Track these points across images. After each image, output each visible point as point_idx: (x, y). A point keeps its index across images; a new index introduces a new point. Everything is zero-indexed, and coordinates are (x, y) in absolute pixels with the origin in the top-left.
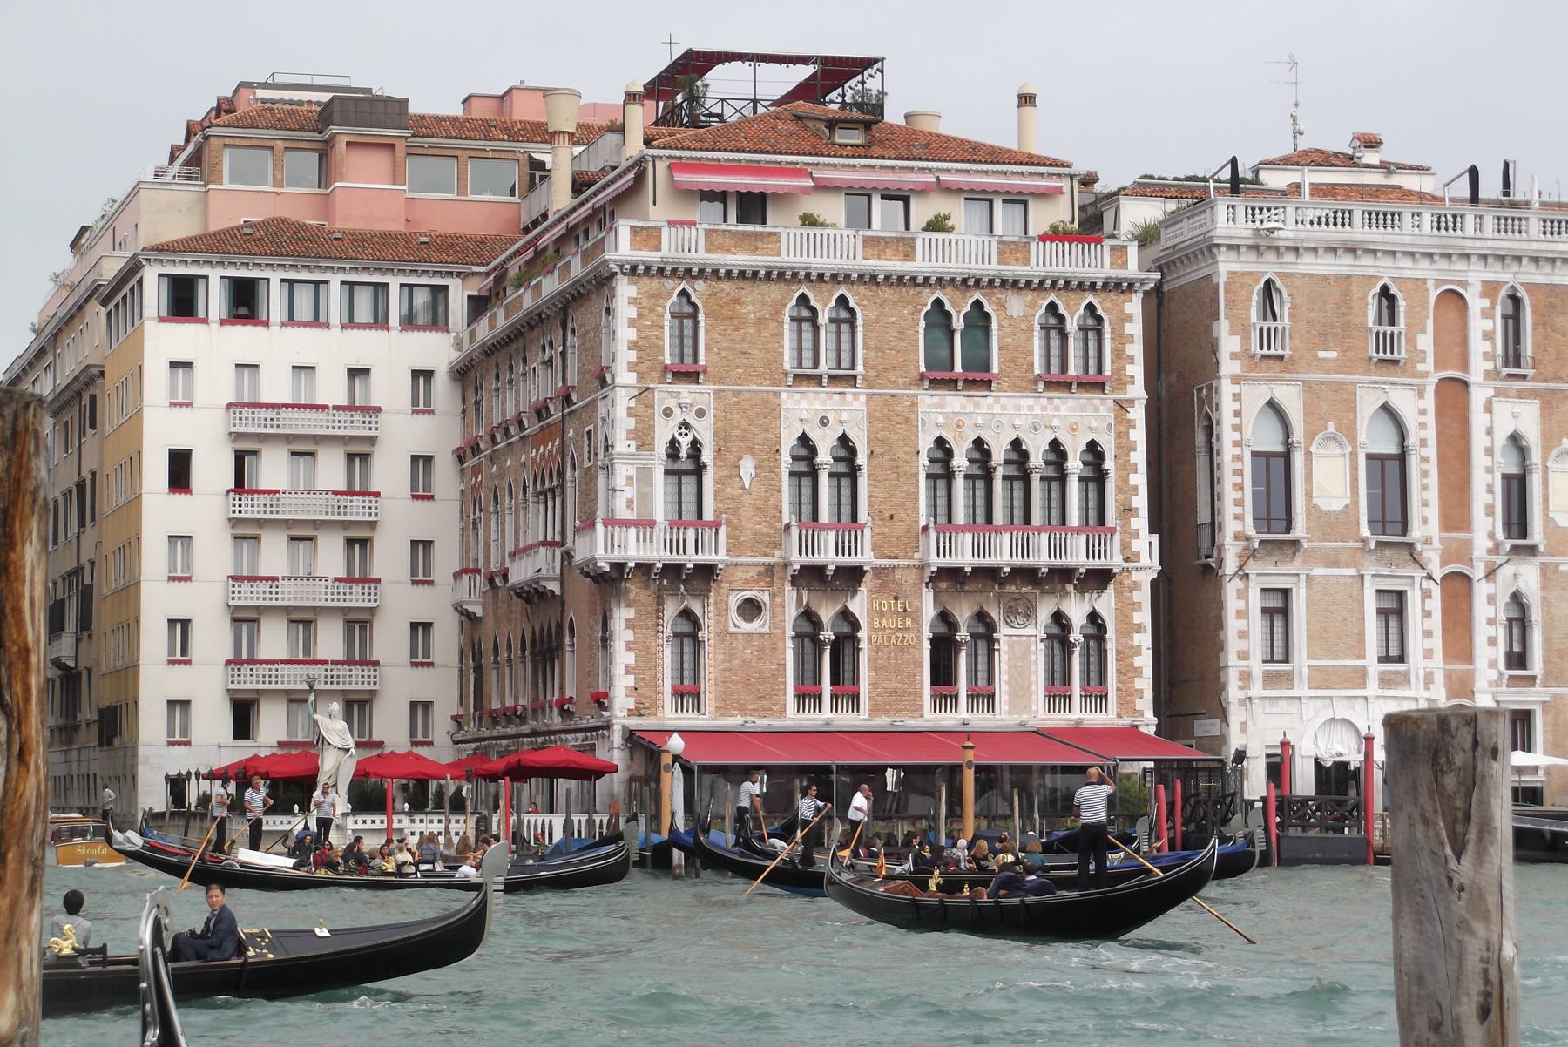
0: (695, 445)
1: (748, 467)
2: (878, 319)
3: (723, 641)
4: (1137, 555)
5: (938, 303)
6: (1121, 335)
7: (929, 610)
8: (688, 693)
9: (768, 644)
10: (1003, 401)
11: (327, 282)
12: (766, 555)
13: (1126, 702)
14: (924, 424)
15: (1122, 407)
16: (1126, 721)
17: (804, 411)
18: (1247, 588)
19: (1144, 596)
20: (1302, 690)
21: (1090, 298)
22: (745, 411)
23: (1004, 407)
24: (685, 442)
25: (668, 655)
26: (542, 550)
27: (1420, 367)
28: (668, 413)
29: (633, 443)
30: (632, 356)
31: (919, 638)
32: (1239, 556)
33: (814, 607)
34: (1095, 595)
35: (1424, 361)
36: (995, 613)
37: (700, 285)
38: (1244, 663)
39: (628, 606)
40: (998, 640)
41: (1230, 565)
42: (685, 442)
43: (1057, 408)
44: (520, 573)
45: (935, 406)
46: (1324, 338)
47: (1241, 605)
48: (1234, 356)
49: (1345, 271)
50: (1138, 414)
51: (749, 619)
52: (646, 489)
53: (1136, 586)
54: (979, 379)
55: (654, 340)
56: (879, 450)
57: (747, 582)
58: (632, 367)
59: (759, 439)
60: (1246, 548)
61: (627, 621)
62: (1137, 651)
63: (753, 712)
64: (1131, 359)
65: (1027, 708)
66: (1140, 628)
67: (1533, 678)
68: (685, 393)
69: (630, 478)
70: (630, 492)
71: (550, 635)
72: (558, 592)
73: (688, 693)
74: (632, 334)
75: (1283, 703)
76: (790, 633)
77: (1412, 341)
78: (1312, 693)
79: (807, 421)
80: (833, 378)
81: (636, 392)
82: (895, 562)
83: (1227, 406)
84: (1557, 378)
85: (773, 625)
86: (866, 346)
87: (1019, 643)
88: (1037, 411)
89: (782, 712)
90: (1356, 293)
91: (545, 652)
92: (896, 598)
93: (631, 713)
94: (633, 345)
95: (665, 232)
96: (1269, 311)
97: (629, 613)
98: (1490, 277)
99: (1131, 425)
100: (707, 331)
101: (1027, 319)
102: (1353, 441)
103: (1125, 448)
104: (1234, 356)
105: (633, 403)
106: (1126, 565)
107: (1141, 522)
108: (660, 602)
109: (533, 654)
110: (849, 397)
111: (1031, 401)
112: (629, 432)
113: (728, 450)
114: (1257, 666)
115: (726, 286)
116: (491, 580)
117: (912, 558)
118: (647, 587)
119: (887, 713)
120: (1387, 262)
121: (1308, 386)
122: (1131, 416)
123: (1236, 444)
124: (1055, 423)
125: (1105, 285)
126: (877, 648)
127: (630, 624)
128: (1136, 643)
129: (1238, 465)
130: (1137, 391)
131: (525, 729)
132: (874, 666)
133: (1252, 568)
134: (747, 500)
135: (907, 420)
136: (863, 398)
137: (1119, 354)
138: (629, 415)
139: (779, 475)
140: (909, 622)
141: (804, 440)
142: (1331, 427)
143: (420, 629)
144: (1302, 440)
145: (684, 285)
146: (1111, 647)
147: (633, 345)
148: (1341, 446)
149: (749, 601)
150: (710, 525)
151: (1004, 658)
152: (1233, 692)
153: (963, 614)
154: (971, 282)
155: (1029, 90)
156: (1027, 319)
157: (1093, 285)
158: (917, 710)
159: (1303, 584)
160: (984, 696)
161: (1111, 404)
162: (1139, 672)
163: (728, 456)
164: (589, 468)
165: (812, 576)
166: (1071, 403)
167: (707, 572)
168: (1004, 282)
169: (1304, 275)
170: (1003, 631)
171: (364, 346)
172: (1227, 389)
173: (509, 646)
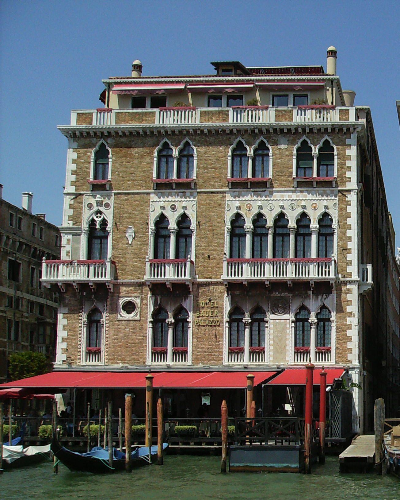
0: (104, 223)
1: (130, 233)
3: (114, 324)
4: (350, 274)
6: (344, 156)
7: (227, 307)
8: (93, 351)
15: (344, 193)
16: (341, 365)
24: (98, 220)
25: (84, 331)
28: (90, 206)
30: (73, 178)
31: (222, 321)
34: (324, 296)
39: (64, 306)
42: (98, 220)
50: (353, 198)
51: (129, 313)
52: (77, 246)
53: (349, 291)
57: (128, 293)
58: (73, 183)
62: (349, 327)
64: (349, 169)
65: (284, 359)
66: (351, 314)
69: (69, 240)
73: (93, 351)
74: (74, 167)
76: (150, 319)
80: (180, 185)
81: (74, 197)
82: (209, 280)
85: (140, 316)
86: (198, 167)
92: (210, 301)
94: (74, 173)
99: (348, 203)
100: (113, 163)
103: (344, 216)
105: (72, 202)
107: (353, 256)
112: (69, 216)
115: (124, 140)
118: (75, 296)
125: (333, 129)
128: (348, 323)
130: (353, 184)
134: (130, 249)
137: (342, 166)
138: (70, 208)
139: (147, 236)
145: (102, 141)
147: (74, 173)
160: (258, 351)
162: (350, 339)
170: (270, 317)
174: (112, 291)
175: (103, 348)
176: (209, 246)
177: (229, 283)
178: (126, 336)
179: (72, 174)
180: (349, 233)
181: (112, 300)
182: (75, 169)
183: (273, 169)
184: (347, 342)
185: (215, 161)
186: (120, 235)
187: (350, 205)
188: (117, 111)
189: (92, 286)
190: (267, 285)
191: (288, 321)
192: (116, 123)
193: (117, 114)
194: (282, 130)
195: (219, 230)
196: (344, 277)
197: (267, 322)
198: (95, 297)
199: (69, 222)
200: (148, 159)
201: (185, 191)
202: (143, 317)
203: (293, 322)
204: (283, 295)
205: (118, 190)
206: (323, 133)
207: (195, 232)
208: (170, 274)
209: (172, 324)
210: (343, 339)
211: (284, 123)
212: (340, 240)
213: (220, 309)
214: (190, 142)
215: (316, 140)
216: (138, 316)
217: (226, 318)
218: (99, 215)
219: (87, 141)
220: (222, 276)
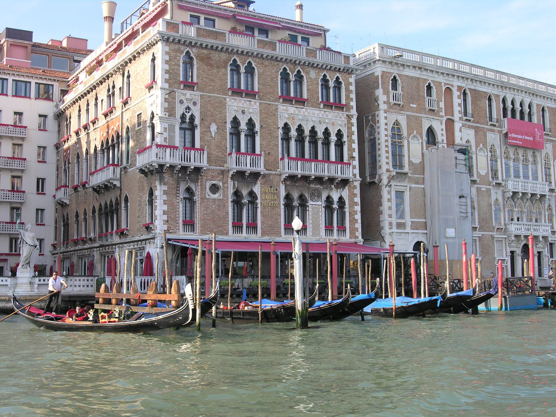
0: (192, 118)
1: (213, 128)
2: (263, 73)
7: (283, 193)
8: (189, 224)
9: (222, 204)
10: (309, 110)
11: (7, 79)
12: (221, 166)
14: (280, 117)
15: (349, 117)
16: (353, 240)
17: (235, 107)
18: (391, 190)
19: (357, 191)
20: (408, 230)
21: (338, 74)
22: (212, 104)
23: (309, 113)
26: (111, 168)
27: (441, 114)
28: (181, 102)
31: (279, 204)
32: (388, 178)
34: (341, 190)
35: (442, 112)
37: (194, 50)
38: (390, 219)
39: (165, 184)
40: (308, 206)
41: (385, 181)
42: (188, 115)
43: (327, 116)
44: (98, 179)
45: (284, 110)
46: (412, 99)
47: (389, 197)
48: (385, 102)
49: (418, 76)
50: (354, 121)
52: (172, 134)
53: (355, 187)
54: (300, 101)
55: (176, 71)
56: (264, 126)
57: (213, 177)
60: (390, 175)
65: (319, 234)
66: (356, 204)
67: (476, 228)
68: (188, 94)
69: (165, 128)
71: (111, 205)
72: (118, 185)
75: (403, 235)
76: (230, 200)
77: (438, 104)
78: (413, 231)
79: (237, 111)
81: (168, 92)
83: (382, 121)
84: (478, 123)
85: (224, 196)
86: (259, 83)
87: (315, 207)
88: (321, 116)
89: (227, 234)
90: (421, 85)
91: (110, 212)
92: (271, 187)
95: (180, 26)
96: (395, 87)
97: (165, 188)
98: (459, 84)
99: (352, 125)
100: (197, 69)
101: (317, 79)
102: (422, 138)
103: (350, 134)
104: (385, 102)
105: (167, 96)
107: (356, 163)
108: (178, 183)
109: (100, 214)
110: (253, 103)
111: (318, 112)
114: (394, 221)
115: (205, 52)
116: (75, 188)
117: (276, 171)
118: (172, 176)
119: (268, 235)
120: (430, 74)
121: (408, 116)
122: (352, 121)
124: (327, 121)
126: (264, 207)
127: (165, 193)
129: (387, 144)
130: (354, 112)
131: (96, 245)
132: (263, 215)
133: (393, 183)
135: (274, 115)
136: (258, 104)
139: (226, 132)
141: (235, 118)
142: (415, 133)
143: (40, 211)
145: (188, 49)
146: (347, 210)
148: (418, 140)
149: (214, 185)
150: (200, 150)
151: (310, 213)
152: (386, 230)
153: (295, 195)
154: (297, 62)
155: (298, 3)
156: (317, 79)
158: (279, 234)
159: (408, 190)
161: (345, 115)
162: (356, 221)
164: (140, 129)
165: (240, 175)
166: (332, 114)
167: (198, 170)
169: (406, 76)
170: (310, 203)
171: (20, 104)
173: (85, 214)
179: (166, 73)
181: (201, 182)
182: (168, 69)
183: (307, 92)
184: (354, 223)
200: (223, 70)
206: (336, 71)
207: (259, 134)
210: (353, 221)
213: (277, 193)
214: (252, 62)
217: (282, 202)
219: (177, 47)
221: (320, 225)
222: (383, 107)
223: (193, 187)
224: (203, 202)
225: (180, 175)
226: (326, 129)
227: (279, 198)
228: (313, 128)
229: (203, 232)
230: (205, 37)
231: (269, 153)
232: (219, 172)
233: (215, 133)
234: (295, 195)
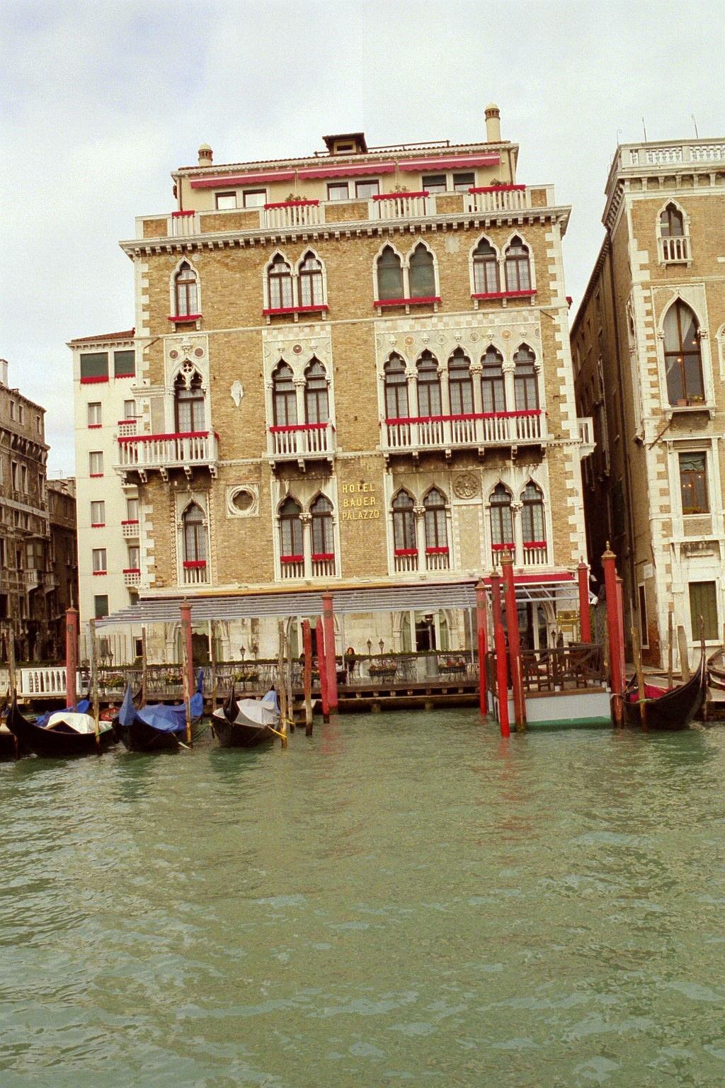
0: (197, 379)
1: (236, 390)
2: (337, 269)
4: (567, 434)
5: (388, 249)
6: (544, 259)
9: (258, 525)
12: (254, 457)
13: (562, 554)
19: (575, 468)
21: (515, 232)
23: (446, 324)
24: (188, 377)
28: (174, 355)
29: (148, 381)
31: (382, 513)
33: (293, 495)
34: (532, 468)
36: (446, 489)
38: (666, 515)
39: (148, 503)
42: (188, 377)
43: (492, 321)
45: (388, 329)
47: (661, 468)
48: (643, 267)
52: (159, 414)
53: (568, 458)
54: (425, 303)
59: (246, 368)
60: (663, 420)
61: (147, 515)
62: (571, 511)
63: (249, 580)
66: (572, 492)
69: (146, 407)
70: (147, 418)
76: (275, 515)
81: (150, 342)
82: (359, 453)
88: (475, 325)
89: (271, 579)
93: (153, 585)
95: (169, 222)
97: (148, 509)
99: (556, 329)
101: (463, 253)
103: (551, 349)
104: (643, 267)
105: (147, 351)
106: (557, 442)
107: (569, 406)
108: (172, 498)
110: (317, 329)
111: (469, 318)
113: (222, 379)
114: (677, 516)
117: (374, 449)
121: (710, 286)
123: (649, 337)
125: (526, 220)
127: (149, 518)
128: (569, 505)
129: (652, 354)
134: (238, 415)
136: (328, 328)
139: (262, 393)
140: (373, 500)
144: (708, 330)
145: (184, 259)
146: (547, 508)
147: (146, 308)
149: (243, 493)
152: (658, 541)
153: (418, 490)
157: (515, 221)
158: (382, 570)
161: (537, 314)
162: (573, 528)
163: (222, 383)
165: (283, 469)
166: (504, 316)
167: (202, 474)
168: (440, 227)
170: (453, 502)
172: (638, 294)
174: (216, 477)
175: (209, 563)
176: (354, 403)
177: (390, 455)
178: (241, 542)
179: (144, 310)
180: (561, 372)
182: (148, 302)
183: (441, 284)
184: (568, 533)
185: (354, 277)
186: (222, 395)
187: (559, 331)
188: (202, 214)
189: (188, 471)
190: (448, 455)
191: (480, 507)
192: (202, 231)
193: (203, 218)
194: (450, 226)
195: (367, 379)
196: (558, 437)
197: (449, 510)
198: (191, 488)
199: (145, 380)
201: (313, 323)
202: (265, 513)
203: (487, 507)
204: (470, 468)
205: (214, 329)
206: (510, 227)
208: (301, 451)
209: (309, 520)
210: (563, 529)
211: (453, 217)
212: (549, 383)
213: (378, 495)
215: (500, 237)
216: (257, 512)
217: (388, 508)
218: (188, 368)
219: (163, 259)
220: (377, 447)
221: (479, 544)
222: (639, 277)
223: (199, 500)
224: (222, 526)
225: (176, 483)
226: (491, 349)
227: (382, 501)
228: (459, 352)
229: (224, 579)
230: (219, 229)
231: (356, 418)
232: (252, 467)
233: (241, 398)
234: (418, 490)
